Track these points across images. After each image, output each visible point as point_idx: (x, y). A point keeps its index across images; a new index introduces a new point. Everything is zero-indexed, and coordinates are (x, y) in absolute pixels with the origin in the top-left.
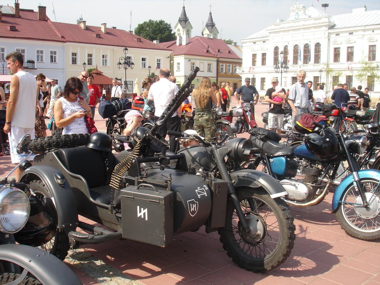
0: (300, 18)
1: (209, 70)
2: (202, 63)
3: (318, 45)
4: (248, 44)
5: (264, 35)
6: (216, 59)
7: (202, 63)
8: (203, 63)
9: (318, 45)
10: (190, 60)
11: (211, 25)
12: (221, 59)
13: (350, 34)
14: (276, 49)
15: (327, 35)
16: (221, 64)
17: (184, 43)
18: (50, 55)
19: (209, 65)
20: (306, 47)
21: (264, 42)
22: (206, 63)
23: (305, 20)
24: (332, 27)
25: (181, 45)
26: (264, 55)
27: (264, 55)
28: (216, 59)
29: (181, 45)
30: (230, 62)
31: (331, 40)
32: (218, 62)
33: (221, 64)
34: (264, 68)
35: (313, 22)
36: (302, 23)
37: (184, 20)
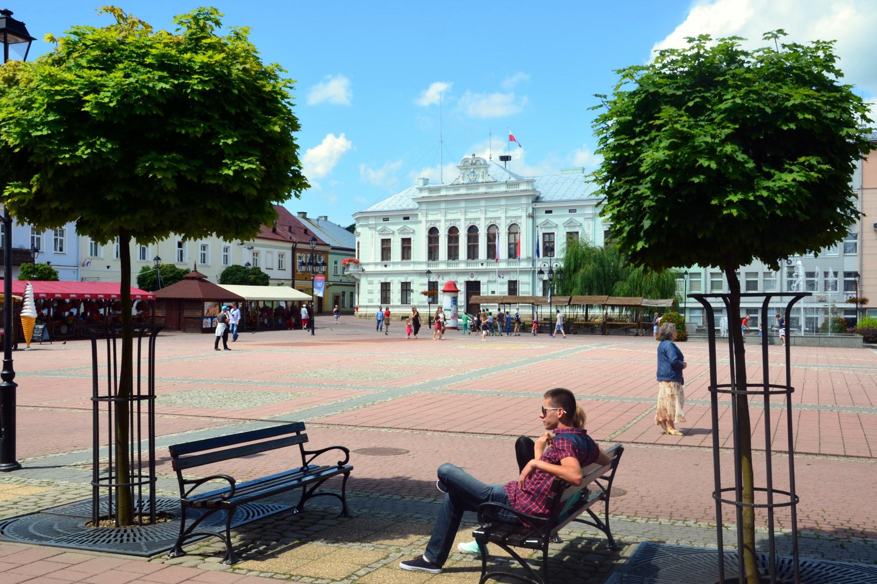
0: (480, 180)
2: (268, 252)
3: (513, 230)
4: (372, 222)
5: (411, 207)
6: (290, 245)
7: (268, 252)
8: (271, 252)
9: (513, 230)
10: (252, 248)
12: (299, 246)
13: (570, 211)
15: (530, 211)
16: (298, 255)
18: (30, 235)
19: (281, 256)
21: (406, 218)
22: (276, 252)
23: (487, 184)
28: (290, 245)
31: (539, 221)
32: (294, 250)
33: (298, 255)
35: (503, 188)
36: (482, 190)
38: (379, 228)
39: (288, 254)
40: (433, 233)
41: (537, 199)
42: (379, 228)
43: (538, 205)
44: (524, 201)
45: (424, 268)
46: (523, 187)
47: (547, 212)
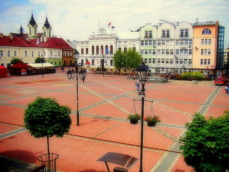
1: (59, 55)
3: (111, 47)
4: (79, 44)
9: (111, 47)
11: (47, 25)
14: (93, 47)
20: (107, 46)
24: (117, 39)
26: (87, 49)
27: (87, 49)
30: (68, 51)
31: (117, 45)
32: (63, 51)
34: (87, 55)
35: (109, 36)
36: (104, 36)
37: (33, 22)
38: (81, 45)
39: (61, 52)
40: (93, 47)
41: (117, 39)
42: (81, 45)
43: (117, 41)
44: (114, 39)
45: (91, 56)
46: (114, 36)
47: (119, 42)
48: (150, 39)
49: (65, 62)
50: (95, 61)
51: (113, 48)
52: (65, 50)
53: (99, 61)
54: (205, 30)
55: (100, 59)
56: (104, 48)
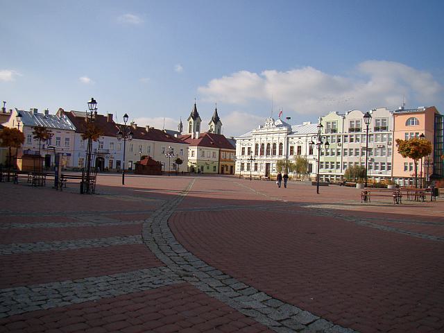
3: (281, 144)
9: (281, 144)
17: (197, 137)
20: (274, 144)
25: (194, 138)
26: (249, 148)
29: (194, 138)
30: (228, 151)
39: (218, 152)
40: (257, 145)
48: (333, 134)
49: (222, 168)
50: (259, 166)
51: (283, 146)
52: (223, 151)
53: (265, 166)
54: (409, 119)
55: (265, 162)
56: (271, 146)
